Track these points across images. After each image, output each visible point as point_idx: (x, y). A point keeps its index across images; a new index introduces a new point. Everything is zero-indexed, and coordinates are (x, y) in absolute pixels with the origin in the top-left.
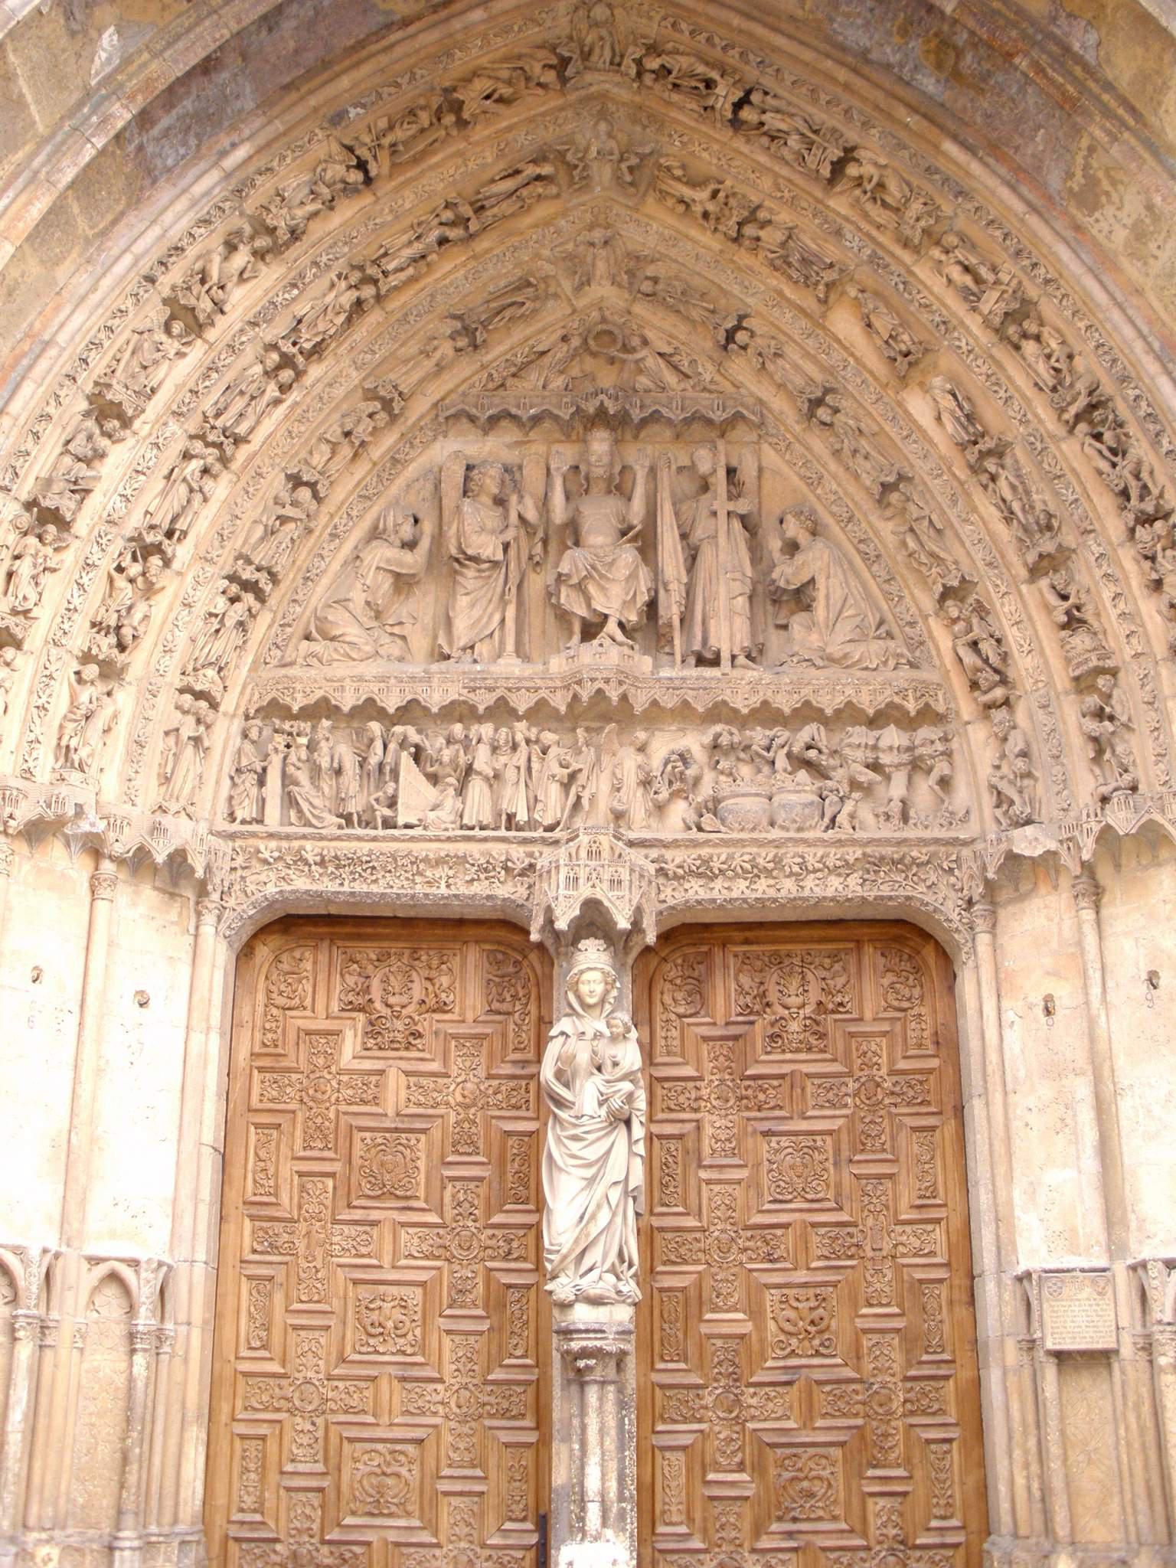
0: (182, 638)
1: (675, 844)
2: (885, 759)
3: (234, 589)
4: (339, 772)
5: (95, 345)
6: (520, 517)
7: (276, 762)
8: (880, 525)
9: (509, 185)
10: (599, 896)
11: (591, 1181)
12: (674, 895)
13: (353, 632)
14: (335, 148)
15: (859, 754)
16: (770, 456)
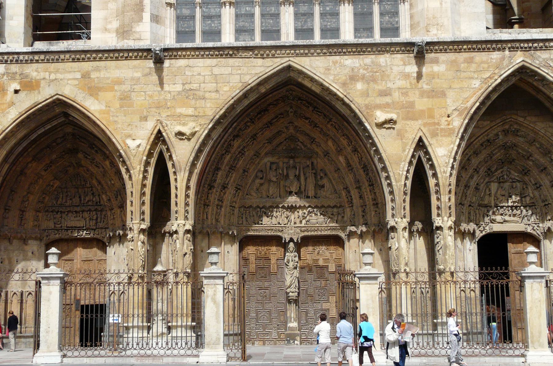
0: (230, 198)
1: (303, 227)
2: (334, 213)
3: (237, 189)
4: (254, 216)
5: (215, 158)
6: (279, 173)
7: (244, 215)
8: (335, 175)
9: (276, 120)
10: (292, 237)
11: (292, 276)
12: (303, 234)
13: (254, 194)
14: (249, 119)
15: (330, 213)
16: (319, 160)
